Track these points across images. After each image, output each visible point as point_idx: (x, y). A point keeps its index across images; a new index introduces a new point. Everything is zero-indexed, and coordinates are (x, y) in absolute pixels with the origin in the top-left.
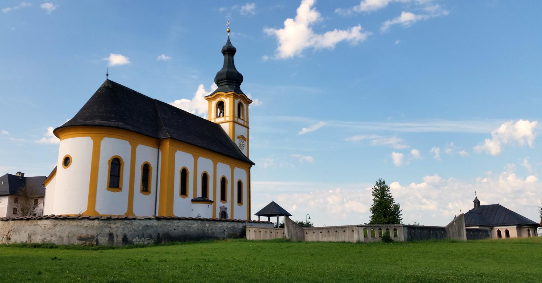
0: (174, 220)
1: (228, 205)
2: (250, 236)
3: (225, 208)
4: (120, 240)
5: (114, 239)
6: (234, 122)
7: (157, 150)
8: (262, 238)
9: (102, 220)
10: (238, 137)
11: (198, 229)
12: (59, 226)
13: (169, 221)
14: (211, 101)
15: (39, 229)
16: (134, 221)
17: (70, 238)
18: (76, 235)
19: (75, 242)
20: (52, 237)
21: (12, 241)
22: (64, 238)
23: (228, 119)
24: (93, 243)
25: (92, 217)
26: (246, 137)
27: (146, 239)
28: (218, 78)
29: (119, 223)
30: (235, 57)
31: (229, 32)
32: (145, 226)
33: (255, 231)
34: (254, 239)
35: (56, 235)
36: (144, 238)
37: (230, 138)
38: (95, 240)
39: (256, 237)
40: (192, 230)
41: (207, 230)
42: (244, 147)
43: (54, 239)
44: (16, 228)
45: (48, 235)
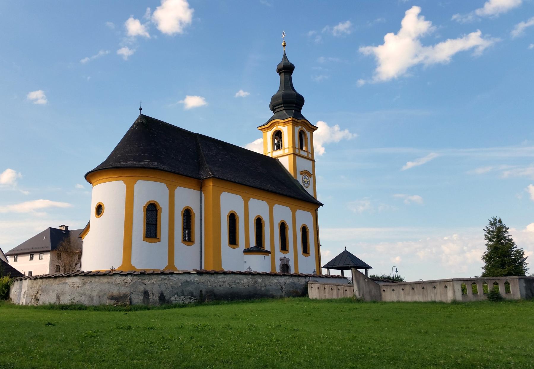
0: (219, 275)
1: (290, 255)
2: (313, 295)
3: (286, 260)
4: (156, 298)
5: (149, 298)
6: (294, 154)
7: (199, 192)
8: (328, 296)
10: (301, 173)
11: (248, 286)
12: (89, 283)
13: (212, 276)
14: (267, 131)
15: (67, 288)
16: (171, 276)
17: (101, 297)
18: (107, 294)
19: (107, 302)
20: (82, 297)
21: (41, 303)
22: (94, 298)
23: (287, 151)
24: (125, 302)
25: (125, 272)
26: (311, 173)
27: (187, 297)
28: (273, 103)
29: (155, 278)
30: (293, 76)
32: (184, 282)
33: (318, 288)
34: (318, 298)
35: (85, 294)
36: (184, 296)
37: (290, 174)
38: (128, 299)
39: (319, 296)
40: (240, 287)
41: (259, 286)
42: (309, 184)
43: (83, 298)
44: (44, 287)
45: (77, 294)
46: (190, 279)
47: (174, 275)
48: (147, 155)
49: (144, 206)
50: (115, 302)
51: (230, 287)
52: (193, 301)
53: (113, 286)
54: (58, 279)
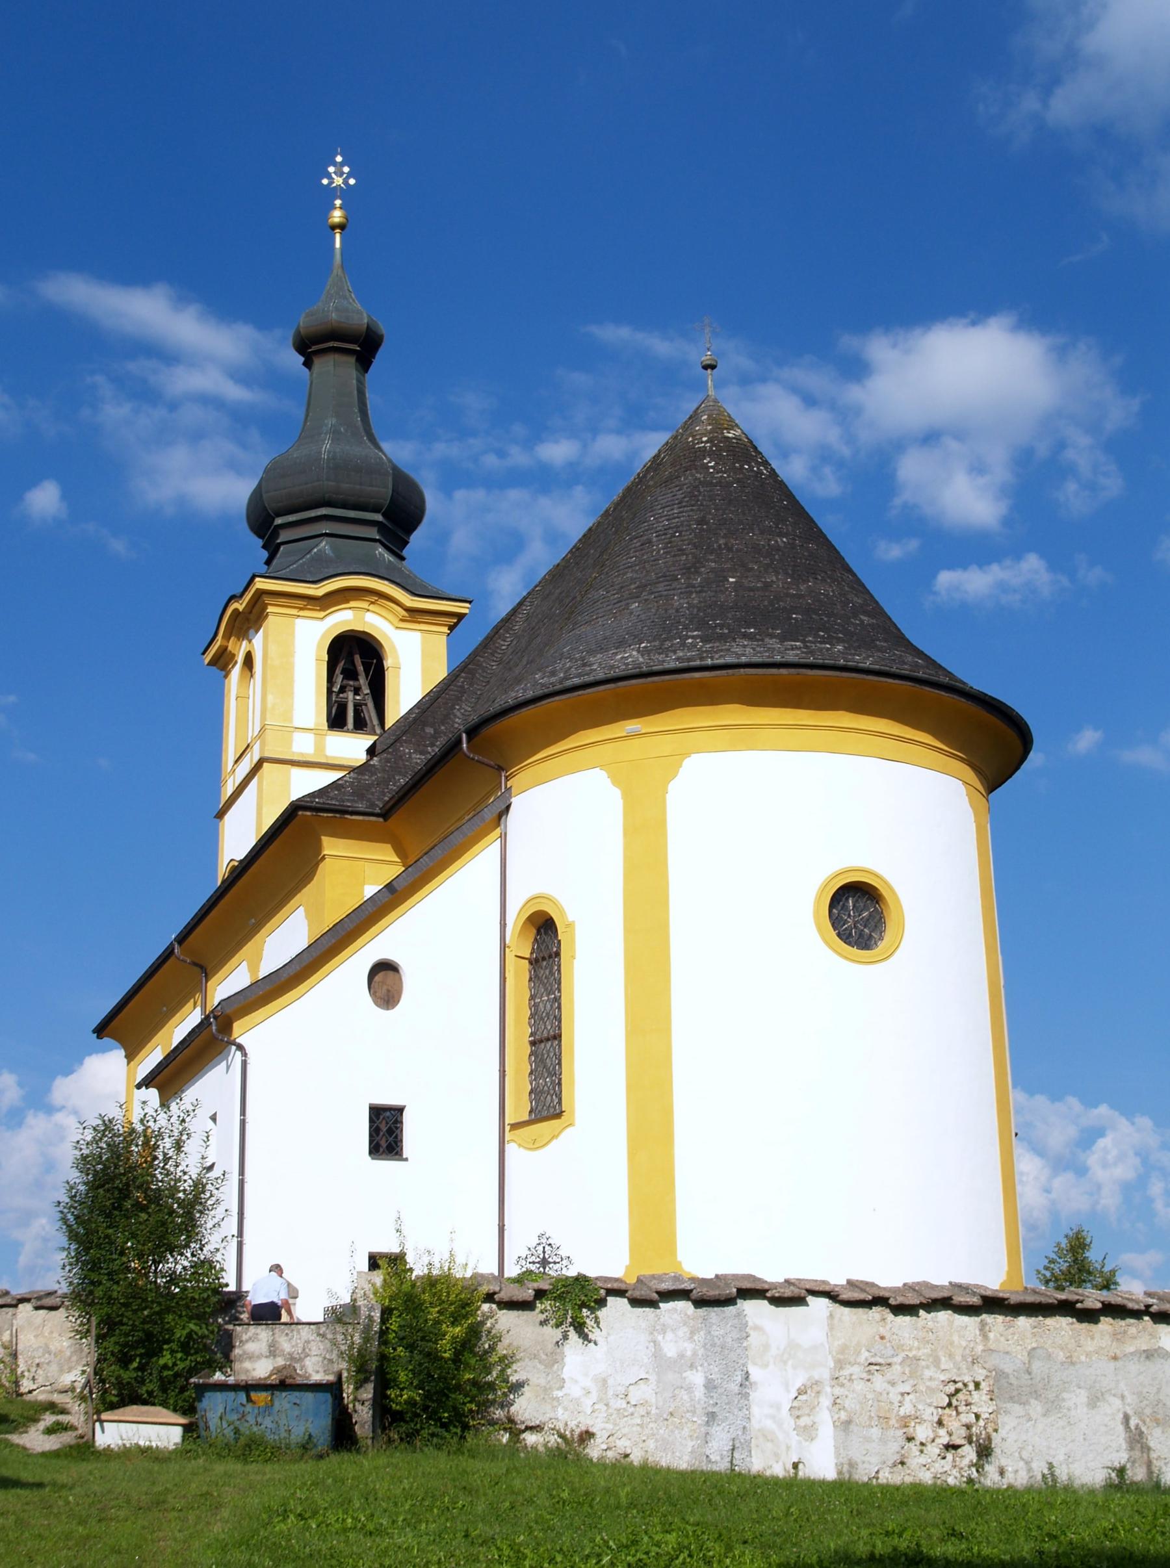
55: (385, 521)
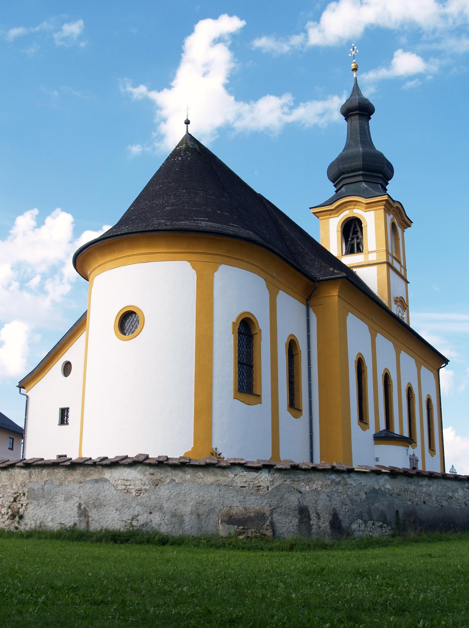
4: (325, 524)
5: (311, 522)
9: (280, 470)
12: (168, 483)
13: (411, 480)
14: (328, 217)
16: (348, 476)
17: (202, 517)
22: (186, 519)
23: (373, 258)
24: (264, 531)
29: (318, 480)
31: (355, 70)
35: (161, 509)
36: (372, 522)
38: (268, 523)
44: (36, 487)
46: (378, 484)
47: (353, 475)
48: (227, 214)
49: (234, 323)
50: (238, 530)
51: (439, 504)
52: (387, 534)
53: (230, 493)
54: (78, 471)
55: (364, 173)
